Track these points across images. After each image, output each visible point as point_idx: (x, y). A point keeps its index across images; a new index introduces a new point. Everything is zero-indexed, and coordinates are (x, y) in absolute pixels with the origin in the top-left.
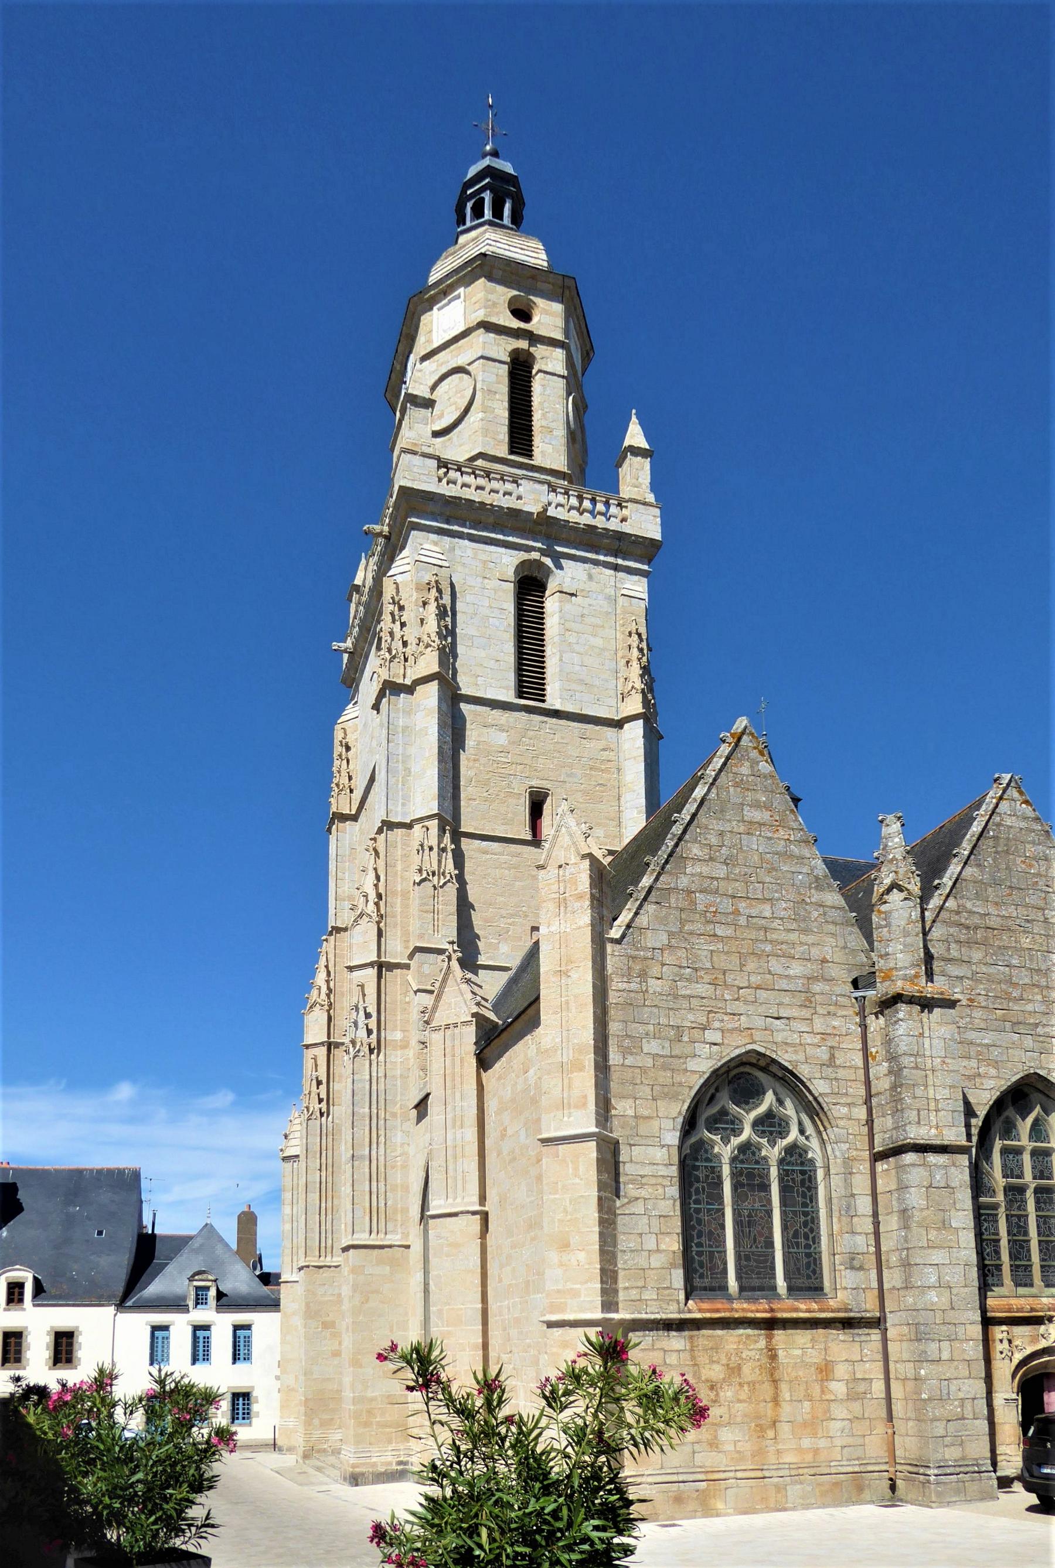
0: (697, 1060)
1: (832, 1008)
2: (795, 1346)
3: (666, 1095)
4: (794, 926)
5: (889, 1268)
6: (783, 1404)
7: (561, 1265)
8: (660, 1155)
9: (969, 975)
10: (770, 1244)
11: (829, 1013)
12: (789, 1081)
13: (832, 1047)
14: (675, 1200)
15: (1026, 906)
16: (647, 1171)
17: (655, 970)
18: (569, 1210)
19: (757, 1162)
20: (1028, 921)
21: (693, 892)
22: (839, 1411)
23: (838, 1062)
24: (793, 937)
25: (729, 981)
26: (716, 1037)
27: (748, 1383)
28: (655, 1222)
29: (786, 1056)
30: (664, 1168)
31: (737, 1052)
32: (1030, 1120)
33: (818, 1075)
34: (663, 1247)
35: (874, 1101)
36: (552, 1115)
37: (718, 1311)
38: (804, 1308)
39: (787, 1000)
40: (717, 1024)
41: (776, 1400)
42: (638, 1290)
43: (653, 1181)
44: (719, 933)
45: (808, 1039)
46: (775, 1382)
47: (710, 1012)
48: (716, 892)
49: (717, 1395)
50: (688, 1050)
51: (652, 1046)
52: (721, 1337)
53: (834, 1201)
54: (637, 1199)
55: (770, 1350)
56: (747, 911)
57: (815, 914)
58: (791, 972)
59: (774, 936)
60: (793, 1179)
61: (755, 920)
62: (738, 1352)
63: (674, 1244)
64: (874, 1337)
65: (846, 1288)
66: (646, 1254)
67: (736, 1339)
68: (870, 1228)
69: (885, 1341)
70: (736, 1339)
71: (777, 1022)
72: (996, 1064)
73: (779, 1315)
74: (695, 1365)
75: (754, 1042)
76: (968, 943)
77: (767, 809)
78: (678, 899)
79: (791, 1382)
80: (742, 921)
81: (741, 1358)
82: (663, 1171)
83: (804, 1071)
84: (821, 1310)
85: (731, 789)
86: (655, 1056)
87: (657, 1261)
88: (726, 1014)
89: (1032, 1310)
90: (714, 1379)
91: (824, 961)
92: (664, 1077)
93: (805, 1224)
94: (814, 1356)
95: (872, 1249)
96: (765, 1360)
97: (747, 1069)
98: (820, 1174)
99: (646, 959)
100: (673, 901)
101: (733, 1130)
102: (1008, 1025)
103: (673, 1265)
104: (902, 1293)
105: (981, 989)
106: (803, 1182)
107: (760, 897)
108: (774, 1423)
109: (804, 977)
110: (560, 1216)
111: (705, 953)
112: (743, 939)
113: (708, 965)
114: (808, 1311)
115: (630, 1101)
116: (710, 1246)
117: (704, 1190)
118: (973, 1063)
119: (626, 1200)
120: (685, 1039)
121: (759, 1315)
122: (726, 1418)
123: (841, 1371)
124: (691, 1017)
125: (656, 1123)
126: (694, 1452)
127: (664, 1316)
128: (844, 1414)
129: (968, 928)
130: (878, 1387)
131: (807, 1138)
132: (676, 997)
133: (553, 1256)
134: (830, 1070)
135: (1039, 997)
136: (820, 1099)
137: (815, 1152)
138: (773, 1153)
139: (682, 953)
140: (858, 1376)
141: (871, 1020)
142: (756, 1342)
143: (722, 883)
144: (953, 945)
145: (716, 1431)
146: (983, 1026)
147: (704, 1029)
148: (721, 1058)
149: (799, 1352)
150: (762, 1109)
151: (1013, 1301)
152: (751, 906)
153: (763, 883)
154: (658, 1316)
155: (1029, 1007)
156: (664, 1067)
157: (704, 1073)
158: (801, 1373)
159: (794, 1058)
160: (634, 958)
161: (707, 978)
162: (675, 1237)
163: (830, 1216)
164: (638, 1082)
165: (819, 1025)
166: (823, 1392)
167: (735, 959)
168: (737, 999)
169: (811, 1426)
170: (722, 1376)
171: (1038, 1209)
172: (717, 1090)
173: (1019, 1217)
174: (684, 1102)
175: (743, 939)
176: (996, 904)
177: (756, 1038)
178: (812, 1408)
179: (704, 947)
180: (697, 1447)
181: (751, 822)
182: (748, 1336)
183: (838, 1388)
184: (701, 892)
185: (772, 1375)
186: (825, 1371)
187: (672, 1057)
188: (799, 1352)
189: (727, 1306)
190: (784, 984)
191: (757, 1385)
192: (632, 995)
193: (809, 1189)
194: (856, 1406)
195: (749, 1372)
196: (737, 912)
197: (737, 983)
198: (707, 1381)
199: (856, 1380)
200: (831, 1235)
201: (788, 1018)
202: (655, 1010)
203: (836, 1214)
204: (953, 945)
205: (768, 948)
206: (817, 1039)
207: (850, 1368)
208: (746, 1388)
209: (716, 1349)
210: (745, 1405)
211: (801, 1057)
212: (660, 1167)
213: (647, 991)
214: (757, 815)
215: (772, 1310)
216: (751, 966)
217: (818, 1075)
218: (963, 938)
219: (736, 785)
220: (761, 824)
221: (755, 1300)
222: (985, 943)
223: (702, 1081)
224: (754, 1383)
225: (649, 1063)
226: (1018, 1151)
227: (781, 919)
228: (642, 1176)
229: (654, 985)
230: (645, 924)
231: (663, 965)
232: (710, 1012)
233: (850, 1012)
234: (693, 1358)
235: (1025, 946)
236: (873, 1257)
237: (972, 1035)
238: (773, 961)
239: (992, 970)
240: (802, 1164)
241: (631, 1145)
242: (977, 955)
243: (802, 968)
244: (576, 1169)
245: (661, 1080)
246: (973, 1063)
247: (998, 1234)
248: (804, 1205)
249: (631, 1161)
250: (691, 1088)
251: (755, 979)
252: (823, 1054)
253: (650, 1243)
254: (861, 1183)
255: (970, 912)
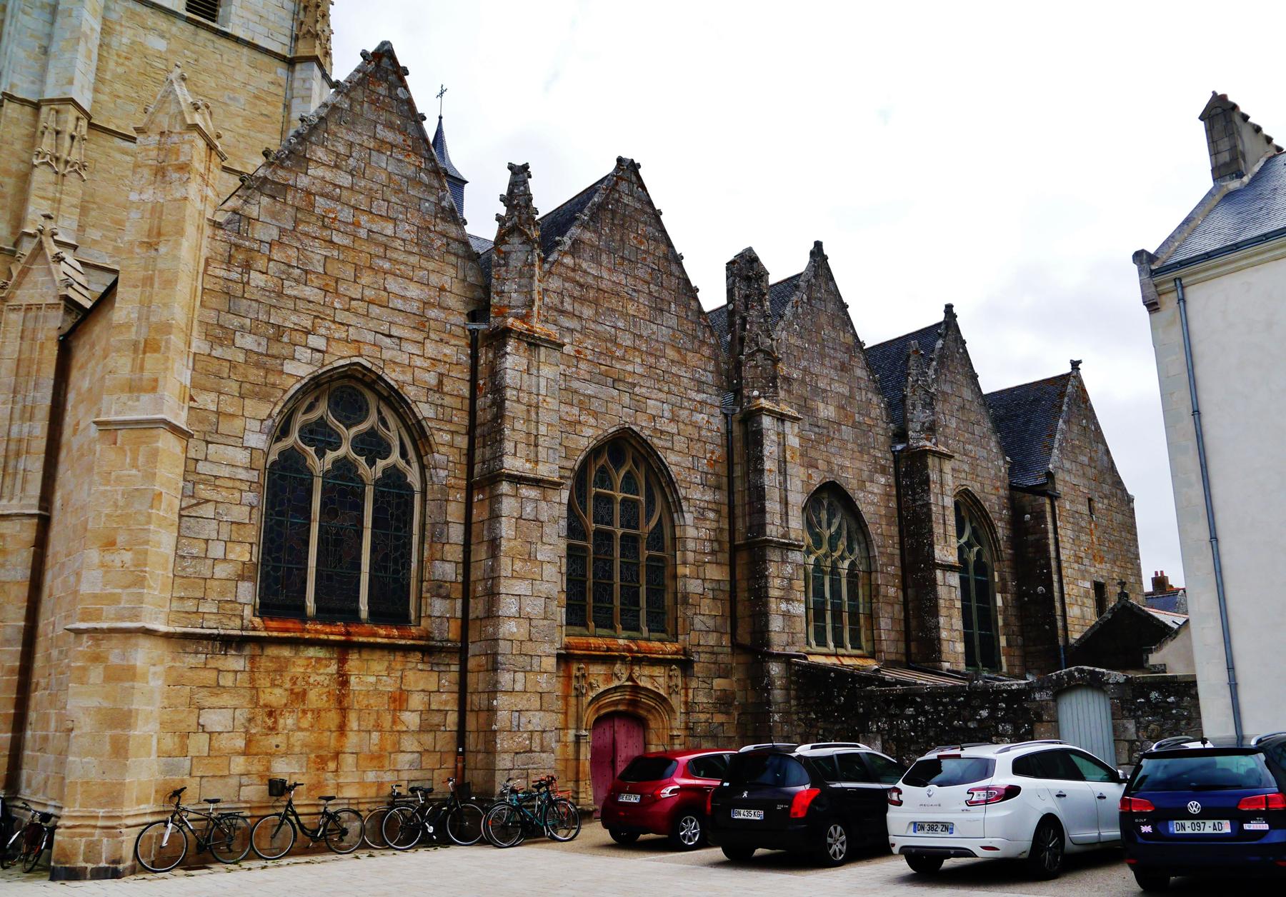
0: (295, 363)
1: (445, 336)
2: (370, 676)
3: (257, 394)
4: (415, 250)
5: (475, 597)
6: (351, 734)
7: (103, 565)
8: (242, 457)
9: (579, 328)
10: (358, 567)
11: (442, 340)
12: (395, 400)
13: (441, 375)
14: (252, 507)
15: (635, 277)
16: (225, 472)
17: (261, 264)
18: (121, 502)
19: (352, 480)
20: (634, 290)
21: (314, 195)
22: (409, 743)
23: (445, 390)
24: (413, 260)
25: (341, 289)
26: (320, 343)
27: (313, 711)
28: (225, 529)
29: (393, 375)
30: (243, 472)
31: (342, 362)
32: (622, 473)
33: (424, 399)
34: (231, 556)
35: (478, 431)
36: (115, 397)
37: (287, 630)
38: (383, 634)
39: (399, 319)
40: (323, 331)
41: (342, 729)
42: (196, 602)
43: (230, 484)
44: (335, 239)
45: (418, 362)
46: (343, 711)
47: (316, 317)
48: (338, 199)
49: (275, 722)
50: (286, 351)
51: (248, 342)
52: (287, 660)
53: (428, 527)
54: (207, 501)
55: (342, 676)
56: (368, 225)
57: (439, 243)
58: (408, 294)
59: (395, 255)
60: (388, 502)
61: (375, 236)
62: (306, 677)
63: (244, 554)
64: (454, 668)
65: (430, 616)
66: (210, 562)
67: (305, 662)
68: (459, 556)
69: (463, 672)
70: (305, 662)
71: (388, 340)
72: (595, 415)
73: (355, 639)
74: (253, 688)
75: (361, 356)
76: (583, 300)
77: (400, 133)
78: (294, 197)
79: (361, 710)
80: (363, 233)
81: (308, 683)
82: (243, 474)
83: (410, 392)
84: (401, 637)
85: (366, 105)
86: (247, 352)
87: (222, 571)
88: (334, 322)
89: (609, 649)
90: (275, 704)
91: (442, 289)
92: (256, 375)
93: (396, 548)
94: (389, 685)
95: (460, 579)
96: (334, 686)
97: (353, 384)
98: (417, 498)
99: (252, 250)
100: (289, 198)
101: (329, 443)
102: (610, 380)
103: (241, 577)
104: (484, 623)
105: (588, 343)
106: (398, 505)
107: (384, 214)
108: (337, 756)
109: (421, 300)
110: (107, 511)
111: (318, 257)
112: (361, 252)
113: (321, 270)
114: (387, 637)
115: (213, 395)
116: (290, 562)
117: (289, 500)
118: (575, 411)
119: (194, 501)
120: (285, 339)
121: (332, 637)
122: (283, 747)
123: (416, 701)
124: (294, 318)
125: (238, 423)
126: (241, 785)
127: (222, 632)
128: (416, 747)
129: (581, 286)
130: (452, 718)
131: (408, 463)
132: (280, 294)
133: (94, 555)
134: (437, 395)
135: (639, 360)
136: (424, 423)
137: (413, 477)
138: (370, 473)
139: (293, 253)
140: (434, 707)
141: (482, 351)
142: (327, 666)
143: (345, 193)
144: (567, 299)
145: (269, 761)
146: (587, 377)
147: (308, 333)
148: (323, 365)
149: (372, 679)
150: (364, 426)
151: (592, 640)
152: (373, 221)
153: (389, 202)
154: (215, 632)
155: (629, 368)
156: (257, 365)
157: (302, 378)
158: (371, 701)
159: (401, 378)
160: (238, 246)
161: (317, 283)
162: (247, 547)
163: (422, 542)
164: (225, 375)
165: (431, 349)
166: (394, 722)
167: (349, 272)
168: (348, 310)
169: (378, 759)
170: (284, 701)
171: (622, 556)
172: (317, 399)
173: (605, 561)
174: (276, 404)
175: (361, 252)
176: (609, 270)
177: (363, 352)
178: (381, 740)
179: (318, 253)
180: (245, 780)
181: (382, 141)
182: (319, 660)
183: (411, 719)
184: (322, 195)
185: (340, 702)
186: (399, 700)
187: (267, 355)
188: (372, 679)
189: (298, 626)
190: (399, 304)
191: (323, 714)
192: (230, 284)
193: (404, 513)
194: (428, 739)
195: (315, 698)
196: (357, 225)
197: (348, 293)
198: (266, 706)
199: (430, 710)
200: (421, 561)
201: (400, 339)
202: (255, 305)
203: (428, 540)
204: (567, 299)
205: (387, 265)
206: (427, 364)
207: (426, 699)
208: (309, 715)
209: (280, 671)
210: (308, 734)
211: (408, 378)
212: (240, 470)
213: (248, 283)
214: (390, 136)
215: (348, 634)
216: (366, 279)
217: (424, 399)
218: (576, 294)
219: (372, 102)
220: (393, 146)
221: (331, 623)
222: (596, 302)
223: (298, 386)
224: (319, 711)
225: (241, 357)
226: (610, 499)
227: (404, 240)
228: (216, 477)
229: (257, 279)
230: (255, 215)
231: (270, 260)
232: (316, 317)
233: (463, 343)
234: (252, 680)
235: (631, 312)
236: (460, 587)
237: (575, 385)
238: (390, 278)
239: (599, 328)
240: (400, 487)
241: (208, 443)
242: (588, 312)
243: (419, 292)
244: (135, 459)
245: (251, 378)
246: (575, 411)
247: (585, 576)
248: (398, 529)
249: (206, 459)
250: (285, 391)
251: (369, 293)
252: (431, 379)
253: (217, 550)
254: (455, 511)
255: (585, 272)
